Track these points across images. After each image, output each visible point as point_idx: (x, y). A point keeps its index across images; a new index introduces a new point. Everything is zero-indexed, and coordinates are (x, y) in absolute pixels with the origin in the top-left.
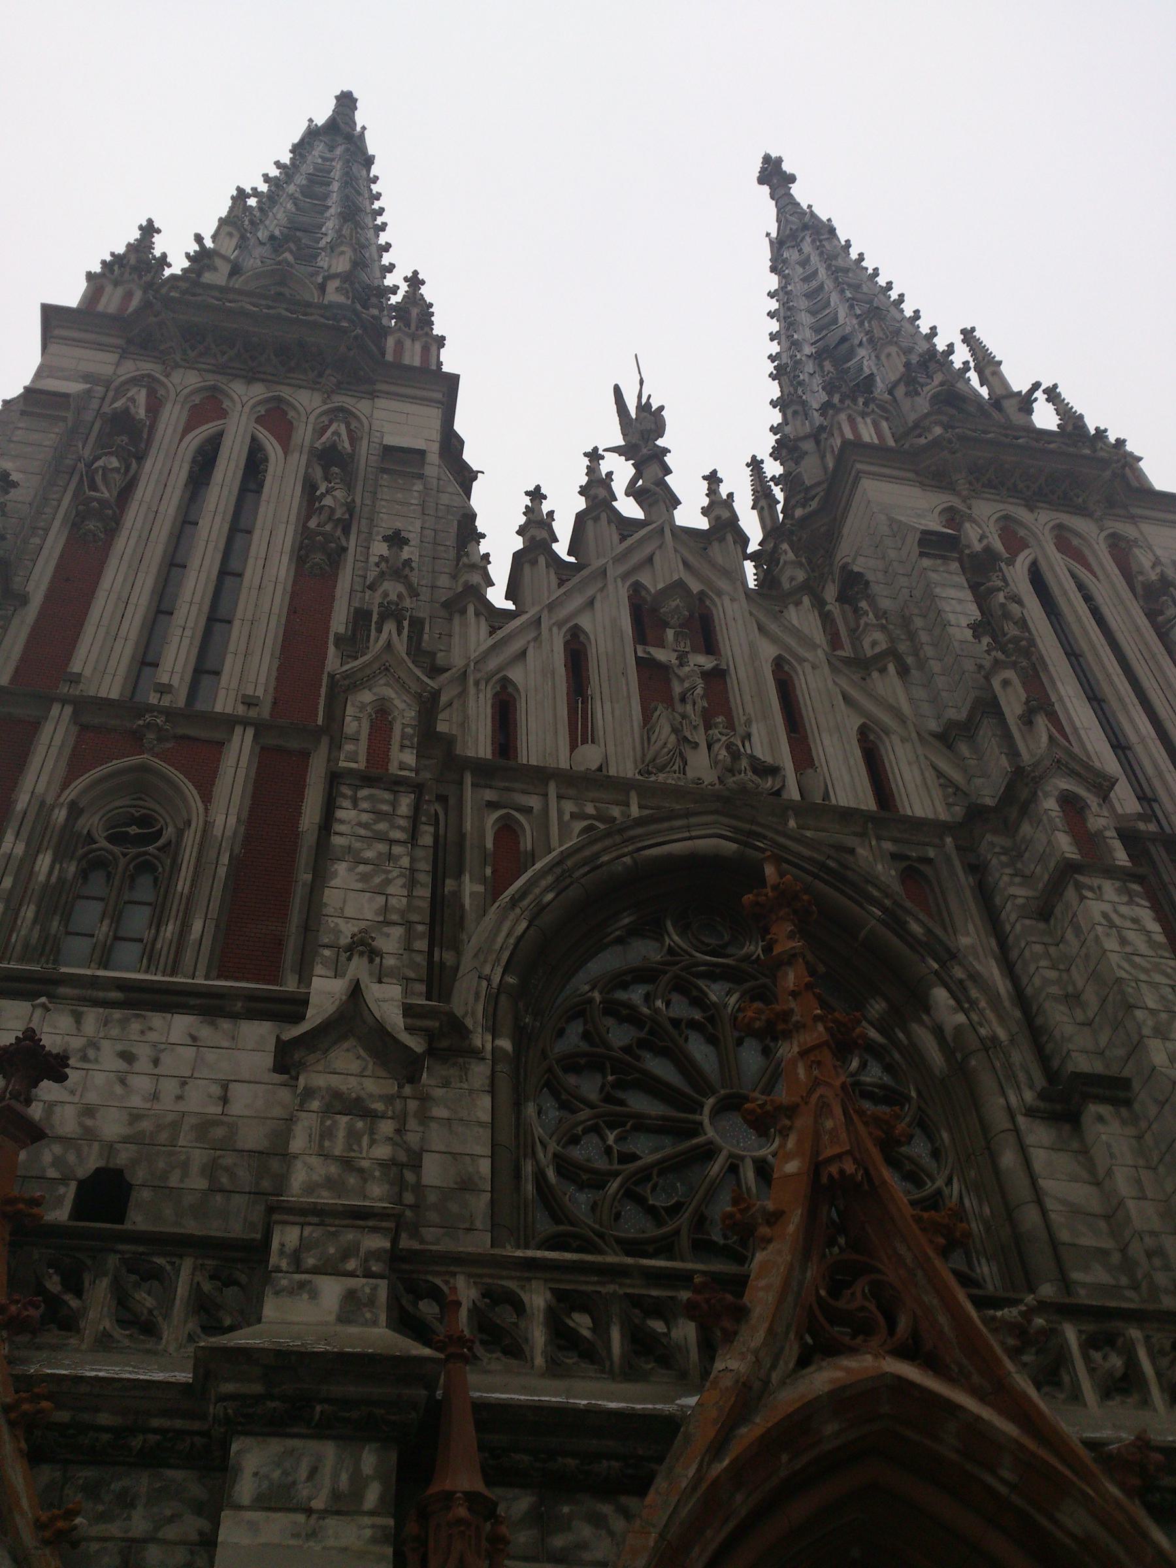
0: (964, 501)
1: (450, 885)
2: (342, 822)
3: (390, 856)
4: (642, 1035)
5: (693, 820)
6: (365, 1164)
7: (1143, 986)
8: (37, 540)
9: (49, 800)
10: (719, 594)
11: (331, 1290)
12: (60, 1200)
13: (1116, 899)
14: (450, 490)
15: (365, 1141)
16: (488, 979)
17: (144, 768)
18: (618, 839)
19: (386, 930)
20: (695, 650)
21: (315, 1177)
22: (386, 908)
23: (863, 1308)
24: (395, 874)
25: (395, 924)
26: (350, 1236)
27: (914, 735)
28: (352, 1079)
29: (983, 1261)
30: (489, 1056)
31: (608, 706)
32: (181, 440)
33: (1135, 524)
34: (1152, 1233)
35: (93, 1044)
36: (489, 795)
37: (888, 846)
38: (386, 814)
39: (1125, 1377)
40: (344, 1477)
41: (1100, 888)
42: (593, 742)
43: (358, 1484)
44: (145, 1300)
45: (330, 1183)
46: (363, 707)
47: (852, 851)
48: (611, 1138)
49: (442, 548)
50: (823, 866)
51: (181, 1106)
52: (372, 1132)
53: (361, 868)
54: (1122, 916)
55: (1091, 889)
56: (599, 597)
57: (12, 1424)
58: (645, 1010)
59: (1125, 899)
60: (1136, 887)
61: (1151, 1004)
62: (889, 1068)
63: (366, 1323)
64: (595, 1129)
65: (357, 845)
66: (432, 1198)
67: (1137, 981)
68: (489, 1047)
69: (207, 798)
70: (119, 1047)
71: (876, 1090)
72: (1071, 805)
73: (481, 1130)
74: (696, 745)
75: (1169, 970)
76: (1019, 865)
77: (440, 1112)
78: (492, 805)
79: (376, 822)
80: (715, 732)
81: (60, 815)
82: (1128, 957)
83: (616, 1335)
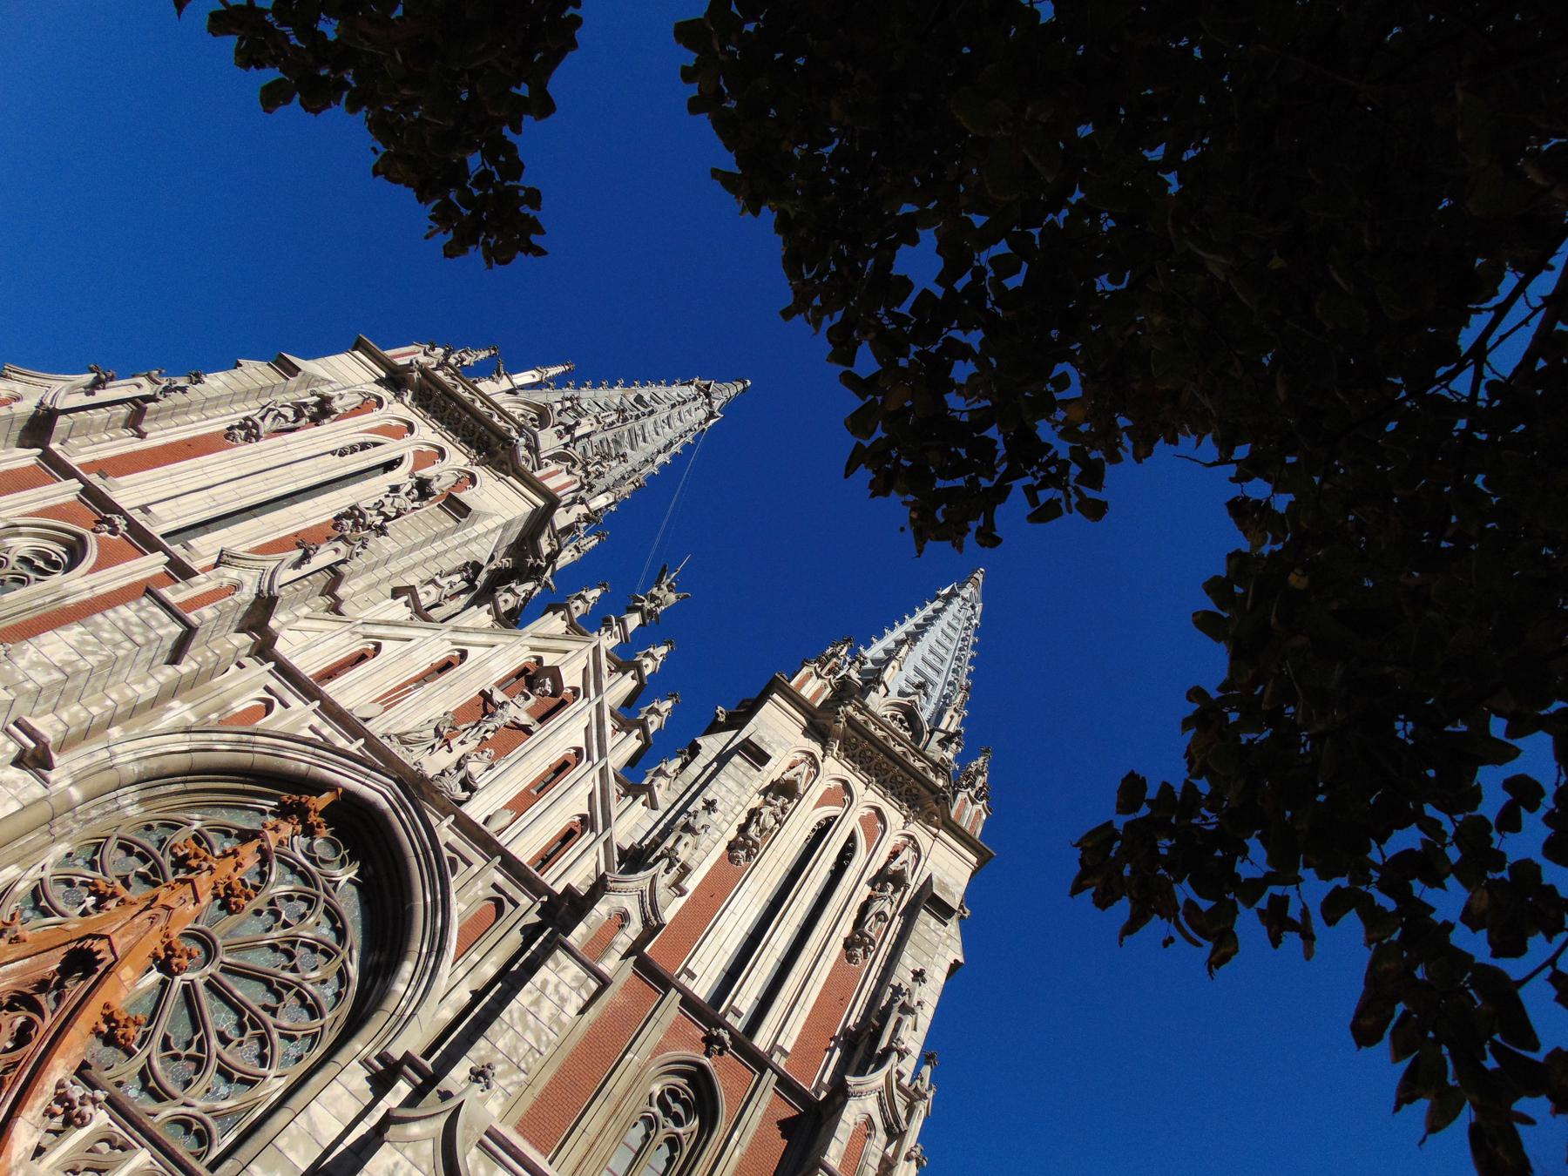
0: (824, 756)
1: (175, 703)
2: (116, 612)
5: (373, 773)
8: (195, 418)
10: (586, 695)
13: (568, 980)
18: (310, 749)
19: (53, 671)
20: (529, 711)
22: (70, 663)
24: (105, 653)
27: (604, 838)
31: (424, 696)
32: (360, 432)
36: (273, 683)
46: (224, 576)
47: (469, 864)
50: (425, 852)
53: (90, 638)
56: (499, 647)
61: (500, 1044)
62: (338, 996)
65: (106, 627)
67: (511, 1027)
69: (93, 570)
71: (309, 998)
74: (450, 751)
75: (544, 1038)
78: (267, 689)
79: (137, 625)
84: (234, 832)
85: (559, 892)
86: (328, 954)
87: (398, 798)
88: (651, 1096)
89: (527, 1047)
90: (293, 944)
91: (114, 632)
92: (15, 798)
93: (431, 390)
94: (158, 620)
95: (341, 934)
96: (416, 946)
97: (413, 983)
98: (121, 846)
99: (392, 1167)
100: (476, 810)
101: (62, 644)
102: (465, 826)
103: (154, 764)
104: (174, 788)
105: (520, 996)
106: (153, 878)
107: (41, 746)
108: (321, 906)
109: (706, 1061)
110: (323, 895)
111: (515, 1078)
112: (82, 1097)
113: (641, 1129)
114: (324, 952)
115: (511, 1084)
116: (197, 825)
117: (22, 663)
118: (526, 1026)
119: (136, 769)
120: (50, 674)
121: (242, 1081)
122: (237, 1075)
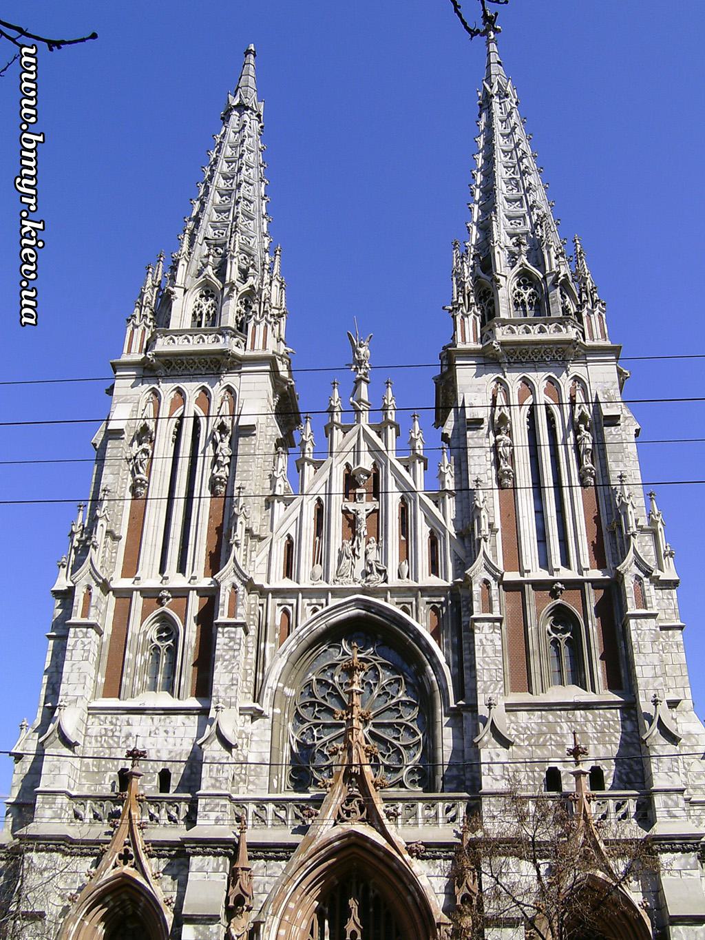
6: (221, 779)
7: (485, 671)
9: (137, 633)
11: (213, 815)
12: (154, 779)
14: (272, 425)
15: (221, 772)
16: (272, 688)
17: (163, 612)
18: (320, 618)
19: (232, 687)
25: (235, 685)
26: (217, 801)
30: (271, 716)
33: (587, 367)
35: (157, 729)
36: (278, 601)
37: (427, 599)
38: (233, 638)
40: (215, 864)
43: (218, 865)
44: (173, 813)
48: (315, 731)
49: (267, 463)
50: (394, 618)
51: (182, 748)
53: (225, 663)
54: (487, 640)
57: (145, 853)
58: (330, 681)
65: (224, 653)
68: (271, 713)
70: (165, 729)
72: (486, 582)
74: (359, 558)
75: (497, 662)
77: (255, 738)
78: (279, 605)
79: (230, 642)
80: (369, 546)
81: (141, 637)
82: (484, 661)
84: (326, 668)
87: (365, 606)
88: (548, 632)
89: (494, 671)
90: (384, 688)
93: (167, 360)
94: (232, 632)
98: (302, 707)
100: (394, 581)
102: (396, 591)
108: (379, 666)
109: (559, 601)
110: (375, 663)
111: (500, 686)
115: (500, 689)
116: (314, 678)
117: (222, 694)
119: (281, 685)
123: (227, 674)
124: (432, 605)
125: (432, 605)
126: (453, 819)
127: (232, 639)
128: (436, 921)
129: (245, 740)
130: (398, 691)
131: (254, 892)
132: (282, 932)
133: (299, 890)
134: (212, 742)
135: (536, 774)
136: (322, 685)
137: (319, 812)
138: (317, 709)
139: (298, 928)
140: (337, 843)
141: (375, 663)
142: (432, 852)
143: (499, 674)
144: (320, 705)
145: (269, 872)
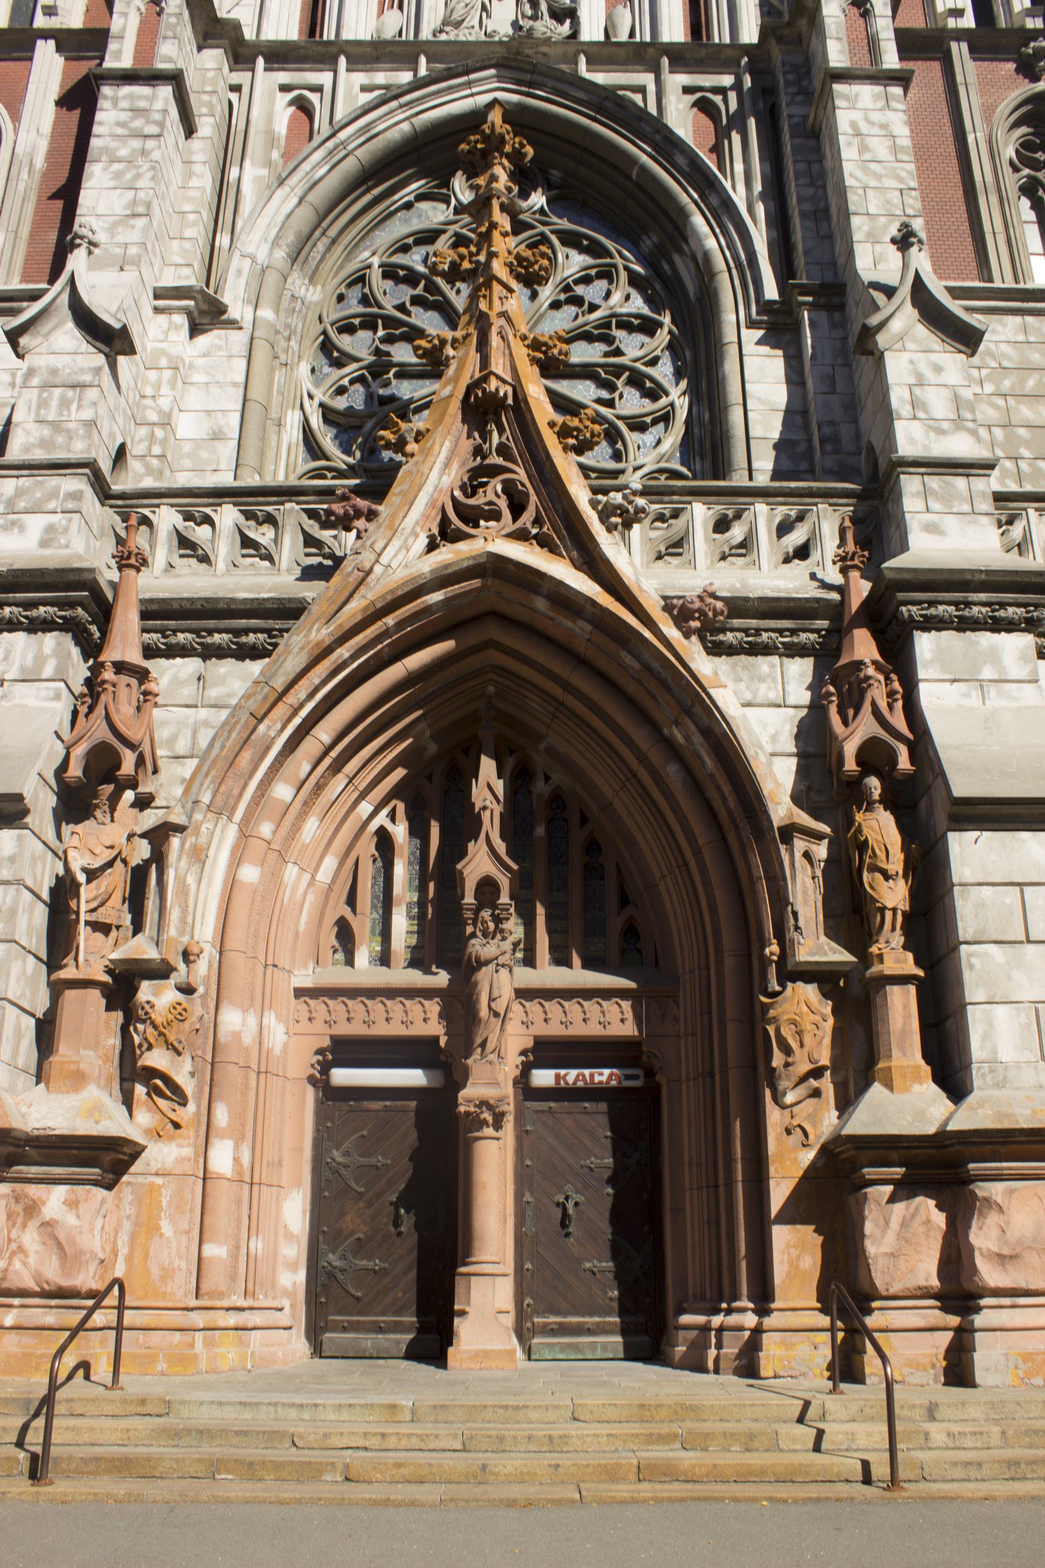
1: (234, 173)
2: (101, 123)
3: (144, 152)
4: (419, 290)
5: (473, 76)
6: (72, 425)
7: (870, 192)
11: (36, 524)
13: (871, 106)
18: (394, 104)
19: (132, 221)
21: (31, 440)
22: (134, 202)
23: (490, 503)
24: (145, 168)
28: (67, 359)
29: (698, 459)
30: (247, 324)
34: (832, 423)
36: (284, 77)
37: (684, 79)
38: (145, 110)
39: (742, 545)
40: (30, 657)
41: (857, 96)
42: (401, 7)
45: (43, 443)
52: (80, 400)
53: (116, 167)
54: (872, 124)
55: (847, 98)
59: (881, 103)
60: (897, 91)
63: (60, 547)
64: (361, 380)
65: (113, 144)
66: (187, 448)
73: (233, 389)
75: (904, 174)
76: (805, 83)
77: (198, 377)
78: (285, 88)
79: (133, 119)
83: (287, 541)
85: (755, 40)
86: (607, 274)
91: (124, 144)
92: (230, 357)
95: (595, 250)
96: (684, 198)
97: (718, 231)
99: (910, 367)
100: (592, 31)
101: (105, 192)
103: (290, 237)
104: (321, 246)
105: (844, 155)
106: (397, 332)
107: (199, 297)
108: (554, 239)
110: (541, 228)
112: (625, 497)
113: (1025, 203)
114: (600, 276)
116: (376, 261)
118: (878, 177)
119: (281, 254)
120: (133, 227)
121: (655, 422)
122: (648, 420)
123: (119, 191)
124: (699, 95)
125: (699, 95)
126: (802, 552)
127: (136, 111)
128: (776, 824)
129: (167, 374)
130: (608, 295)
131: (159, 753)
132: (250, 873)
133: (310, 747)
134: (53, 329)
135: (1023, 465)
136: (398, 280)
137: (380, 508)
138: (381, 333)
139: (306, 877)
140: (436, 597)
141: (546, 230)
142: (746, 631)
143: (911, 201)
144: (390, 322)
145: (213, 693)
